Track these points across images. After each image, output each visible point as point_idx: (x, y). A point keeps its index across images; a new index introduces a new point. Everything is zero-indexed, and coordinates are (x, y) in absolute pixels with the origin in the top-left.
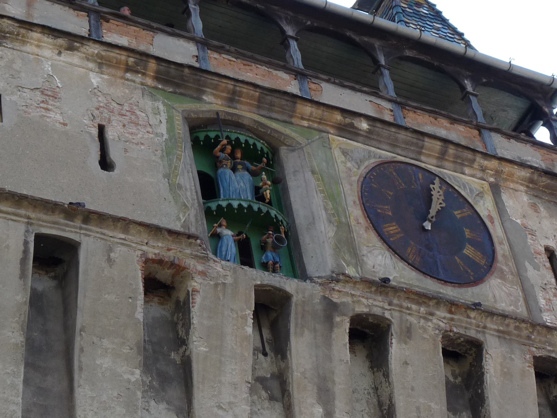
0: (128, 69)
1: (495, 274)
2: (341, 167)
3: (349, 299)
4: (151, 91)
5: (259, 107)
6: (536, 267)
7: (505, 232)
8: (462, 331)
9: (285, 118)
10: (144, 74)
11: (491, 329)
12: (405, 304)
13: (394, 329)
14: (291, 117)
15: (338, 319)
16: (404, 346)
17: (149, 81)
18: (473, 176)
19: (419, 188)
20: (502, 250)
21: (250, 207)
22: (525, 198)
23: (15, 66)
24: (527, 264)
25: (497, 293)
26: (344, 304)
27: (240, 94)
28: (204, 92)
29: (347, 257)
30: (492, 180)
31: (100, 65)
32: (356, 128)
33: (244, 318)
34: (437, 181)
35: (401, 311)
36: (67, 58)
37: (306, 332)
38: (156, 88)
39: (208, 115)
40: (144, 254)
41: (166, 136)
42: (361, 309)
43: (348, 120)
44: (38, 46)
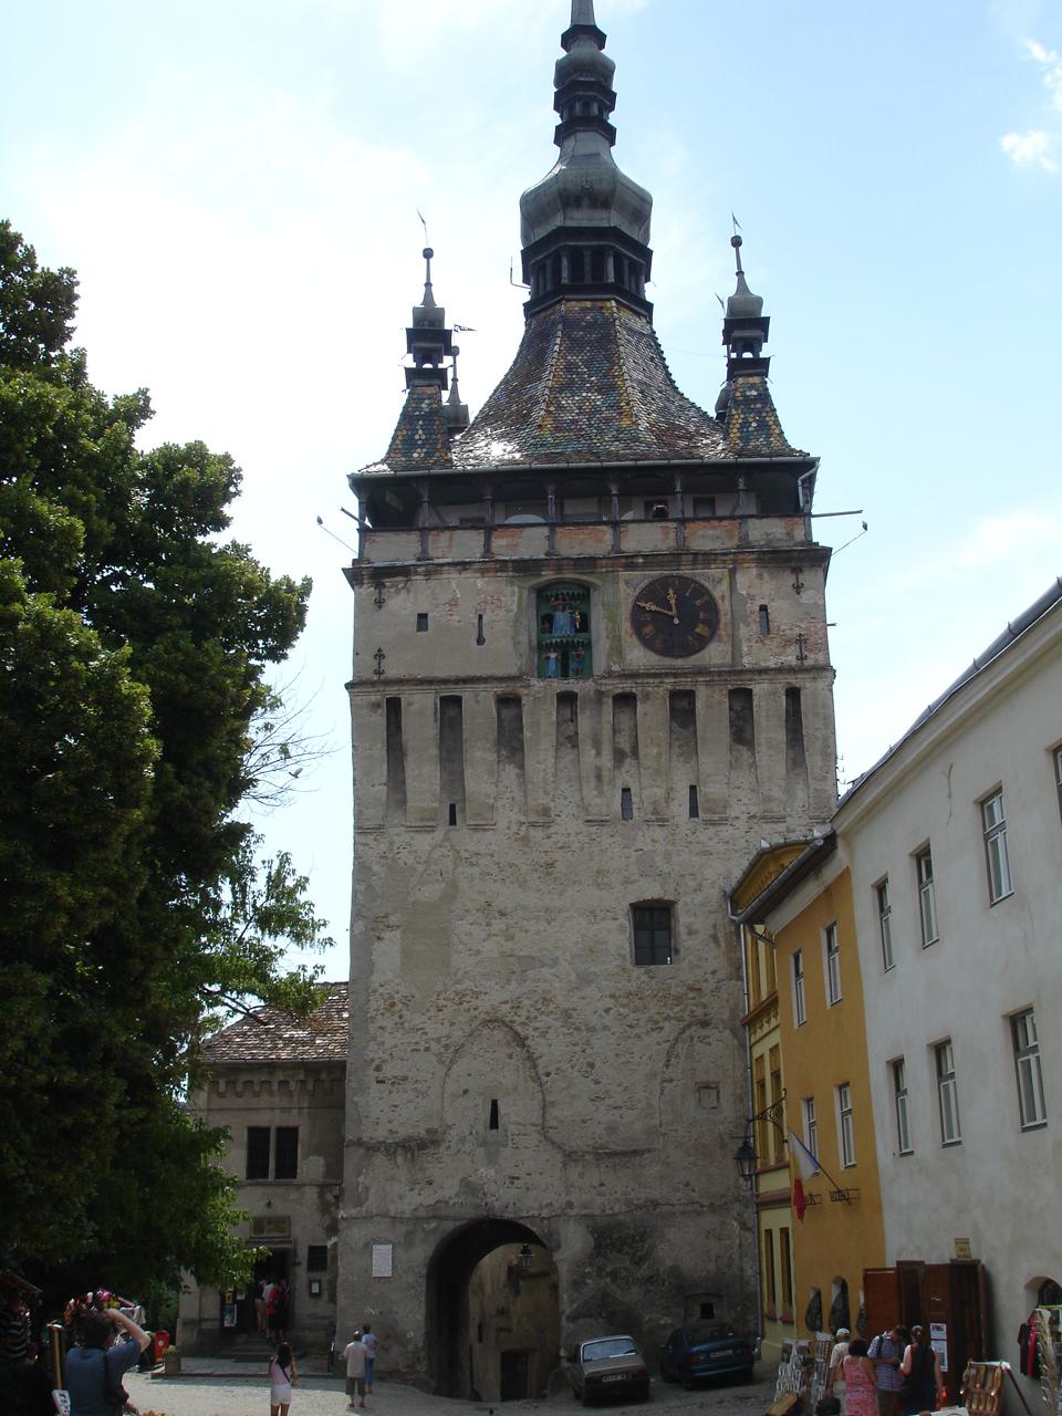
0: (497, 571)
2: (623, 595)
3: (611, 687)
6: (748, 625)
15: (604, 700)
17: (511, 574)
20: (724, 619)
22: (754, 571)
24: (741, 625)
25: (712, 654)
26: (609, 690)
29: (615, 659)
31: (483, 573)
33: (551, 713)
41: (516, 609)
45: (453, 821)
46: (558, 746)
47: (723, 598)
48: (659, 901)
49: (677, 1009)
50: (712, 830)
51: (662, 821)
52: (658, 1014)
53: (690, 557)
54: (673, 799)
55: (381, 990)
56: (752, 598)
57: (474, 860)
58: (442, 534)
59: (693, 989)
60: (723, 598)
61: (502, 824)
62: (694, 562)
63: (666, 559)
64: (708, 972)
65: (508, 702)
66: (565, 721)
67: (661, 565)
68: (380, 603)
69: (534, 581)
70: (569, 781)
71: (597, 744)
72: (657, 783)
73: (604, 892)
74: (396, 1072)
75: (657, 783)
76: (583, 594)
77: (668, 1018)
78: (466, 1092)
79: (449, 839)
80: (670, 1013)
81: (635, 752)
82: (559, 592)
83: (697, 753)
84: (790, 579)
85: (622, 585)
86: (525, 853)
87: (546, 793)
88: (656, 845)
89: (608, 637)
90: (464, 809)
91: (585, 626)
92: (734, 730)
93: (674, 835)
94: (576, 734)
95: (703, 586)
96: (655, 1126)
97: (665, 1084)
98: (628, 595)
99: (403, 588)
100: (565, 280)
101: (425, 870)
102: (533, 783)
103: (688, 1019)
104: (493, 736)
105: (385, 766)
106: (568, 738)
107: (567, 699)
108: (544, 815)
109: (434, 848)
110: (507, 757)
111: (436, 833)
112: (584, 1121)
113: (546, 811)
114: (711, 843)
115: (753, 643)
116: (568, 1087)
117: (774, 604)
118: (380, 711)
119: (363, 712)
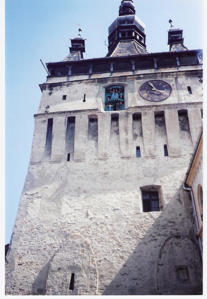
0: (92, 82)
1: (171, 96)
4: (96, 85)
5: (119, 80)
7: (177, 87)
8: (159, 110)
9: (125, 80)
10: (95, 82)
11: (166, 108)
12: (145, 109)
13: (142, 114)
14: (126, 80)
16: (145, 117)
17: (96, 83)
18: (171, 77)
19: (155, 84)
21: (118, 100)
22: (184, 78)
23: (70, 89)
27: (115, 79)
28: (107, 82)
30: (175, 77)
31: (87, 84)
32: (141, 77)
34: (149, 82)
35: (144, 110)
36: (81, 84)
37: (122, 120)
38: (98, 84)
39: (108, 86)
40: (88, 114)
41: (97, 92)
42: (134, 112)
43: (138, 76)
44: (75, 84)
45: (68, 160)
46: (111, 133)
47: (173, 85)
48: (153, 187)
49: (163, 231)
50: (174, 160)
51: (153, 157)
52: (155, 233)
53: (160, 74)
54: (157, 149)
55: (28, 223)
56: (184, 85)
57: (75, 172)
58: (74, 77)
59: (170, 222)
60: (173, 85)
61: (87, 160)
62: (162, 76)
63: (151, 75)
64: (178, 214)
65: (93, 120)
66: (114, 126)
67: (150, 78)
68: (50, 94)
69: (105, 85)
70: (116, 145)
71: (126, 130)
72: (151, 144)
73: (129, 183)
74: (28, 260)
75: (151, 144)
76: (121, 90)
77: (159, 235)
78: (59, 269)
79: (66, 165)
80: (160, 232)
81: (141, 134)
82: (113, 88)
83: (166, 134)
84: (199, 79)
85: (136, 84)
86: (96, 169)
87: (106, 148)
88: (151, 165)
89: (131, 97)
90: (73, 155)
91: (123, 98)
92: (181, 127)
93: (158, 162)
94: (118, 130)
95: (165, 82)
96: (155, 289)
97: (159, 266)
98: (138, 86)
99: (59, 89)
100: (120, 36)
101: (55, 176)
102: (101, 145)
103: (169, 235)
104: (86, 129)
105: (45, 141)
106: (115, 131)
107: (115, 118)
108: (105, 156)
109: (59, 168)
110: (92, 138)
111: (61, 164)
112: (118, 286)
113: (105, 155)
114: (174, 164)
115: (186, 96)
116: (109, 268)
117: (192, 86)
118: (45, 123)
119: (39, 124)
